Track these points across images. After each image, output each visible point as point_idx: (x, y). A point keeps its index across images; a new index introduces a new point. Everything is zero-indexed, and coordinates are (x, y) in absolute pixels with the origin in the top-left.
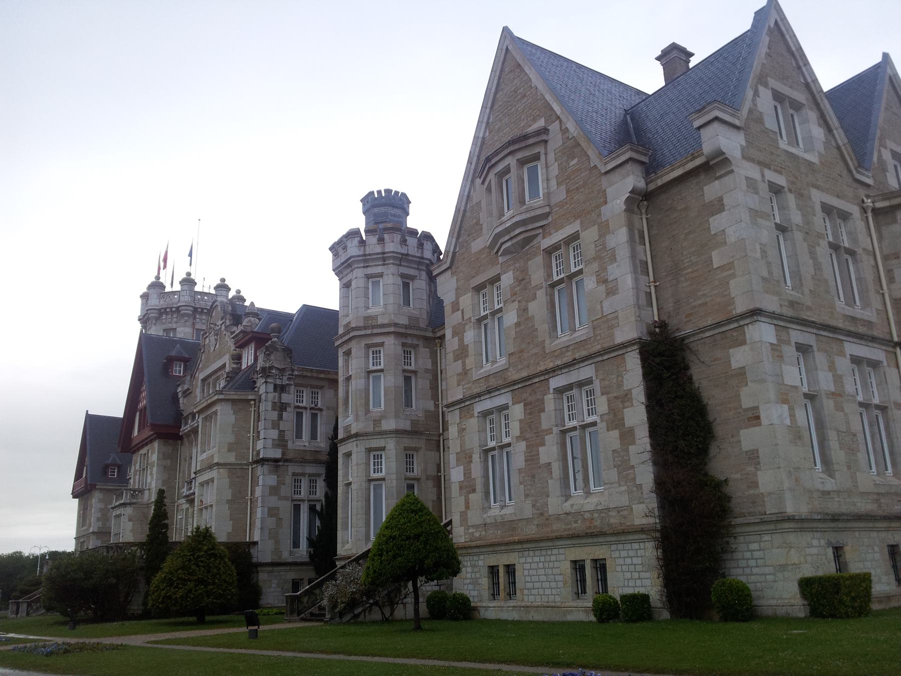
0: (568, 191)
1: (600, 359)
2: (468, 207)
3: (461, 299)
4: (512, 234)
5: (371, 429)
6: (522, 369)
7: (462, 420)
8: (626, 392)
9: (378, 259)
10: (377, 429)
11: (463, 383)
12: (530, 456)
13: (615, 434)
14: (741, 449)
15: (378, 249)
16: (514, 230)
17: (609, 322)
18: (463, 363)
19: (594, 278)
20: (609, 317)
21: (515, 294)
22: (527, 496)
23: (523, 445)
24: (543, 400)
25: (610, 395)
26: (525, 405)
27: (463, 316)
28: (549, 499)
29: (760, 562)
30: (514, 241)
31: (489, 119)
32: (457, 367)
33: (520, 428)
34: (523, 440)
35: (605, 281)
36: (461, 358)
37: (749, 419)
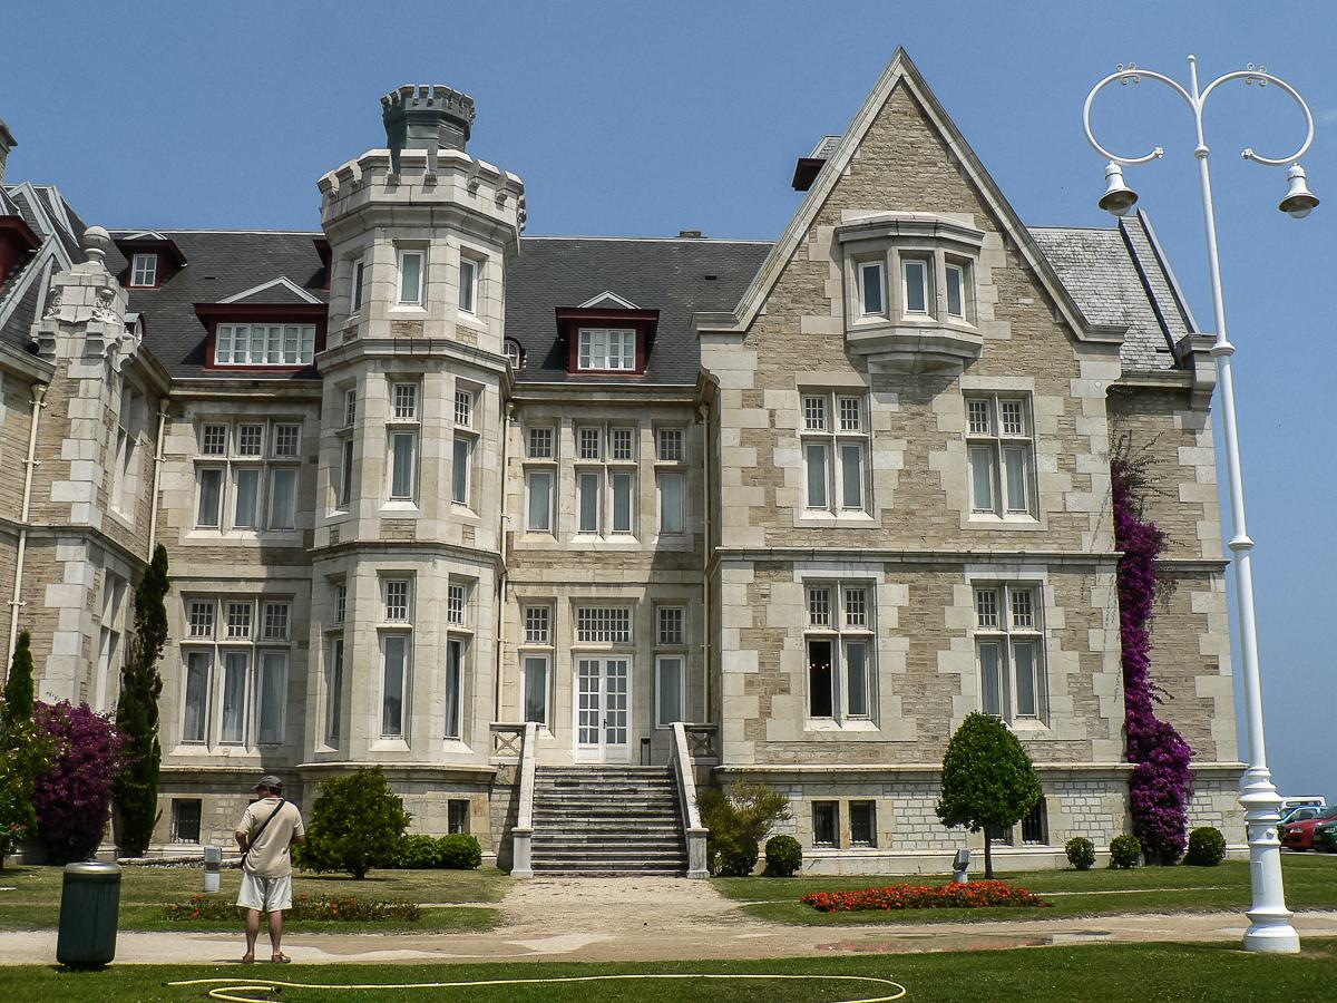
0: (1014, 332)
1: (1058, 562)
2: (795, 258)
3: (768, 394)
4: (923, 348)
5: (457, 541)
6: (909, 537)
7: (759, 580)
8: (1094, 611)
9: (484, 229)
10: (468, 545)
11: (767, 524)
12: (919, 659)
13: (1074, 655)
14: (1195, 694)
15: (495, 213)
16: (927, 344)
17: (1078, 523)
18: (767, 492)
19: (1055, 461)
20: (1075, 515)
21: (902, 429)
22: (907, 712)
23: (905, 643)
24: (951, 588)
25: (1068, 609)
26: (911, 588)
27: (773, 423)
28: (952, 720)
29: (1206, 808)
30: (919, 357)
31: (855, 152)
32: (757, 495)
33: (900, 618)
34: (904, 636)
35: (1072, 470)
36: (761, 484)
37: (1207, 666)
